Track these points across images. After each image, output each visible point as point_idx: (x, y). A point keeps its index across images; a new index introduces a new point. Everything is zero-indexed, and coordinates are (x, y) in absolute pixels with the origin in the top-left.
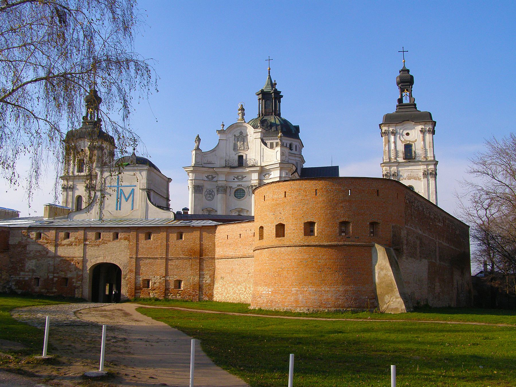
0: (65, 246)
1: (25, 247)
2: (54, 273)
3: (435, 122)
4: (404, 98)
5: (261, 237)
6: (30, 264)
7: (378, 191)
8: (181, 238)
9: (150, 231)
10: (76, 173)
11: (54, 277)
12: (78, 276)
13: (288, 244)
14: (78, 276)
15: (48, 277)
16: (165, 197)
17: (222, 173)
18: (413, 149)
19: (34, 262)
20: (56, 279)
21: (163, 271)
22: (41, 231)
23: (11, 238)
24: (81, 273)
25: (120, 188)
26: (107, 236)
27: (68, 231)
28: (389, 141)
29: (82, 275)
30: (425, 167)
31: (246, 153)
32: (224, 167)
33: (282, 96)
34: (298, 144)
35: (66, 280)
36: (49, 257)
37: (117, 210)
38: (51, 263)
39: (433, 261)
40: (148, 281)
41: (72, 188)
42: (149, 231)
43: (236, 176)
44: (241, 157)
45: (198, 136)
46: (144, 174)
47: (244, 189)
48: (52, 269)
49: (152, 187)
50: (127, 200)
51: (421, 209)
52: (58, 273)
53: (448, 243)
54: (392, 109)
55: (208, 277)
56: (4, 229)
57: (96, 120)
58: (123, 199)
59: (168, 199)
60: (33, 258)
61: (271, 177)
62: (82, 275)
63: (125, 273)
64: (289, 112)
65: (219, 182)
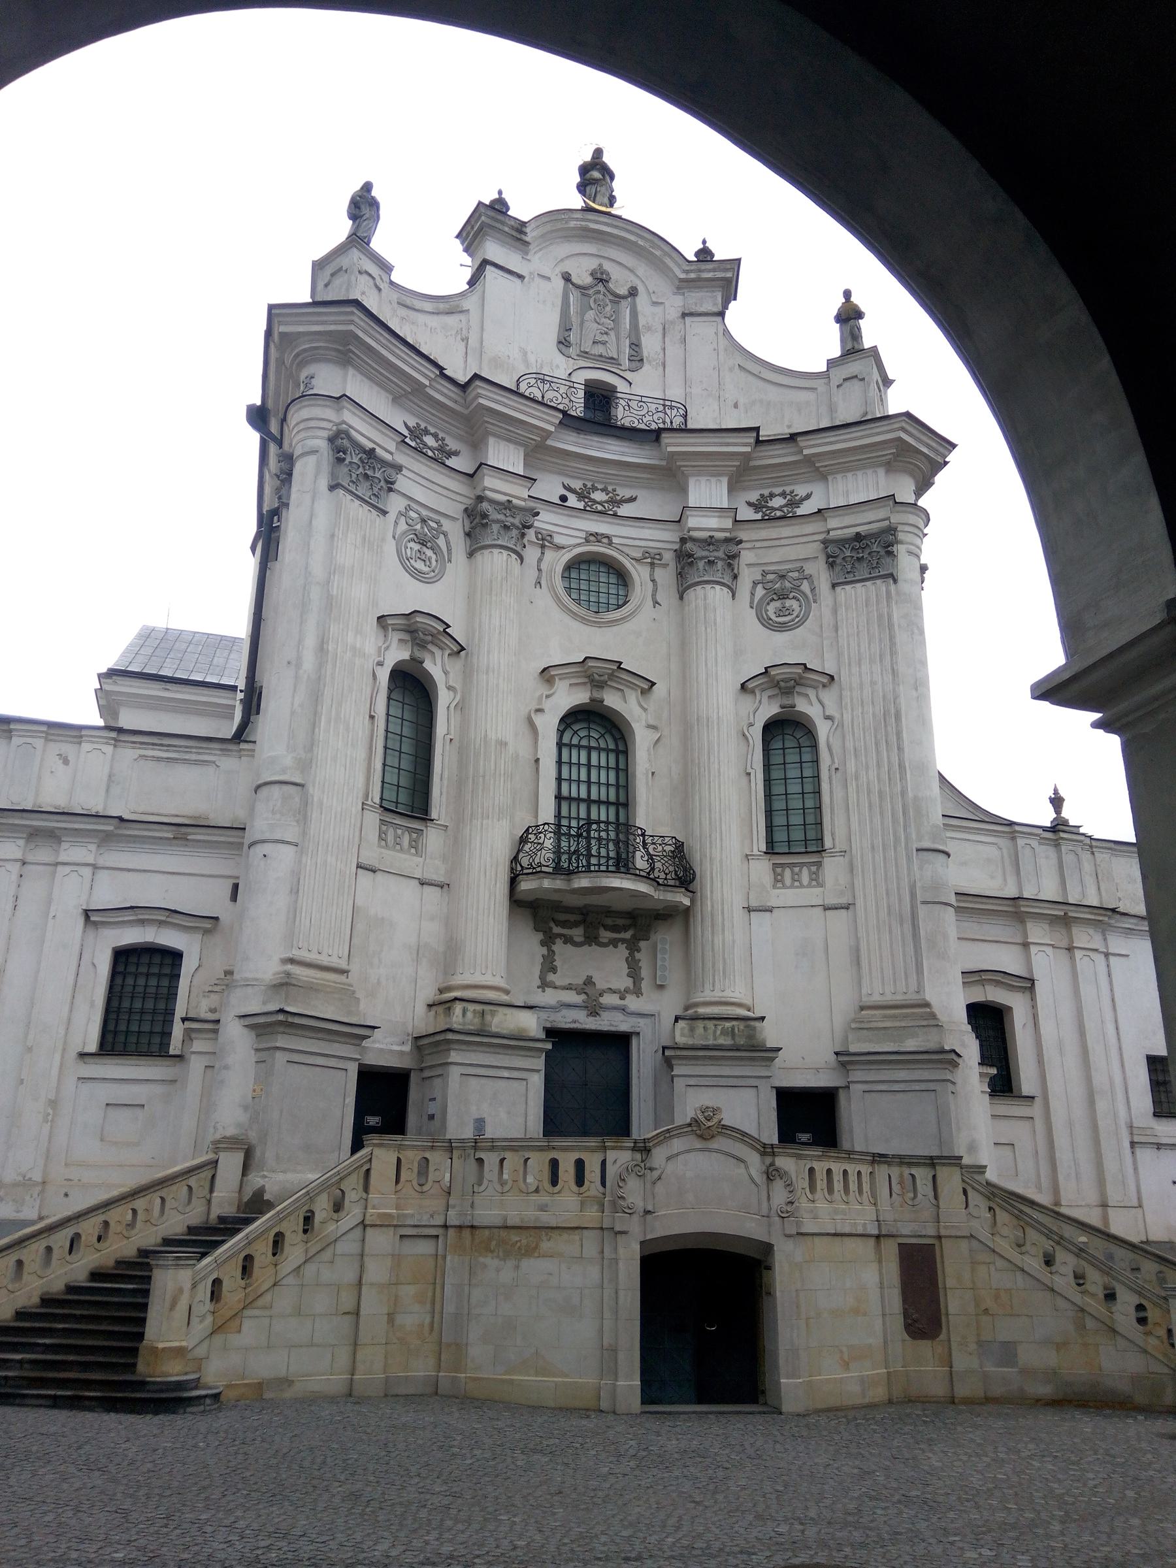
17: (512, 430)
43: (577, 485)
44: (600, 398)
45: (367, 187)
61: (805, 509)
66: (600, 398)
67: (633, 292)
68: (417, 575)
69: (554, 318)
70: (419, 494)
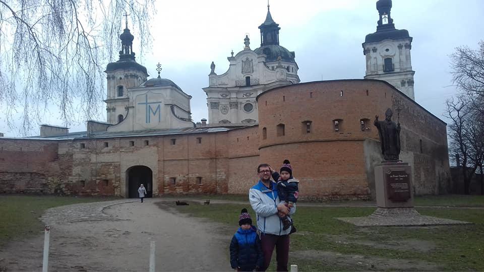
0: (105, 154)
1: (71, 155)
2: (96, 176)
3: (412, 38)
4: (383, 20)
5: (265, 137)
6: (76, 170)
7: (367, 91)
8: (200, 143)
9: (174, 138)
10: (117, 97)
11: (96, 179)
12: (116, 177)
13: (288, 141)
14: (116, 177)
15: (92, 179)
16: (187, 111)
17: (233, 91)
18: (393, 63)
19: (79, 168)
20: (98, 181)
21: (185, 171)
22: (84, 142)
23: (60, 149)
24: (118, 175)
25: (148, 105)
26: (138, 143)
27: (106, 142)
28: (370, 57)
29: (120, 177)
30: (403, 77)
31: (252, 74)
32: (235, 87)
33: (280, 28)
34: (294, 66)
35: (107, 181)
36: (92, 163)
37: (147, 122)
38: (94, 168)
39: (418, 153)
40: (175, 179)
41: (114, 109)
42: (173, 138)
44: (248, 78)
46: (168, 91)
47: (252, 104)
48: (95, 174)
49: (175, 103)
50: (154, 114)
51: (406, 107)
52: (100, 176)
53: (430, 138)
54: (373, 30)
55: (223, 173)
56: (53, 142)
57: (130, 53)
58: (152, 114)
59: (189, 113)
60: (79, 165)
62: (120, 177)
63: (155, 174)
64: (285, 41)
65: (232, 99)
66: (248, 78)
67: (252, 60)
68: (224, 114)
69: (241, 68)
70: (223, 103)
